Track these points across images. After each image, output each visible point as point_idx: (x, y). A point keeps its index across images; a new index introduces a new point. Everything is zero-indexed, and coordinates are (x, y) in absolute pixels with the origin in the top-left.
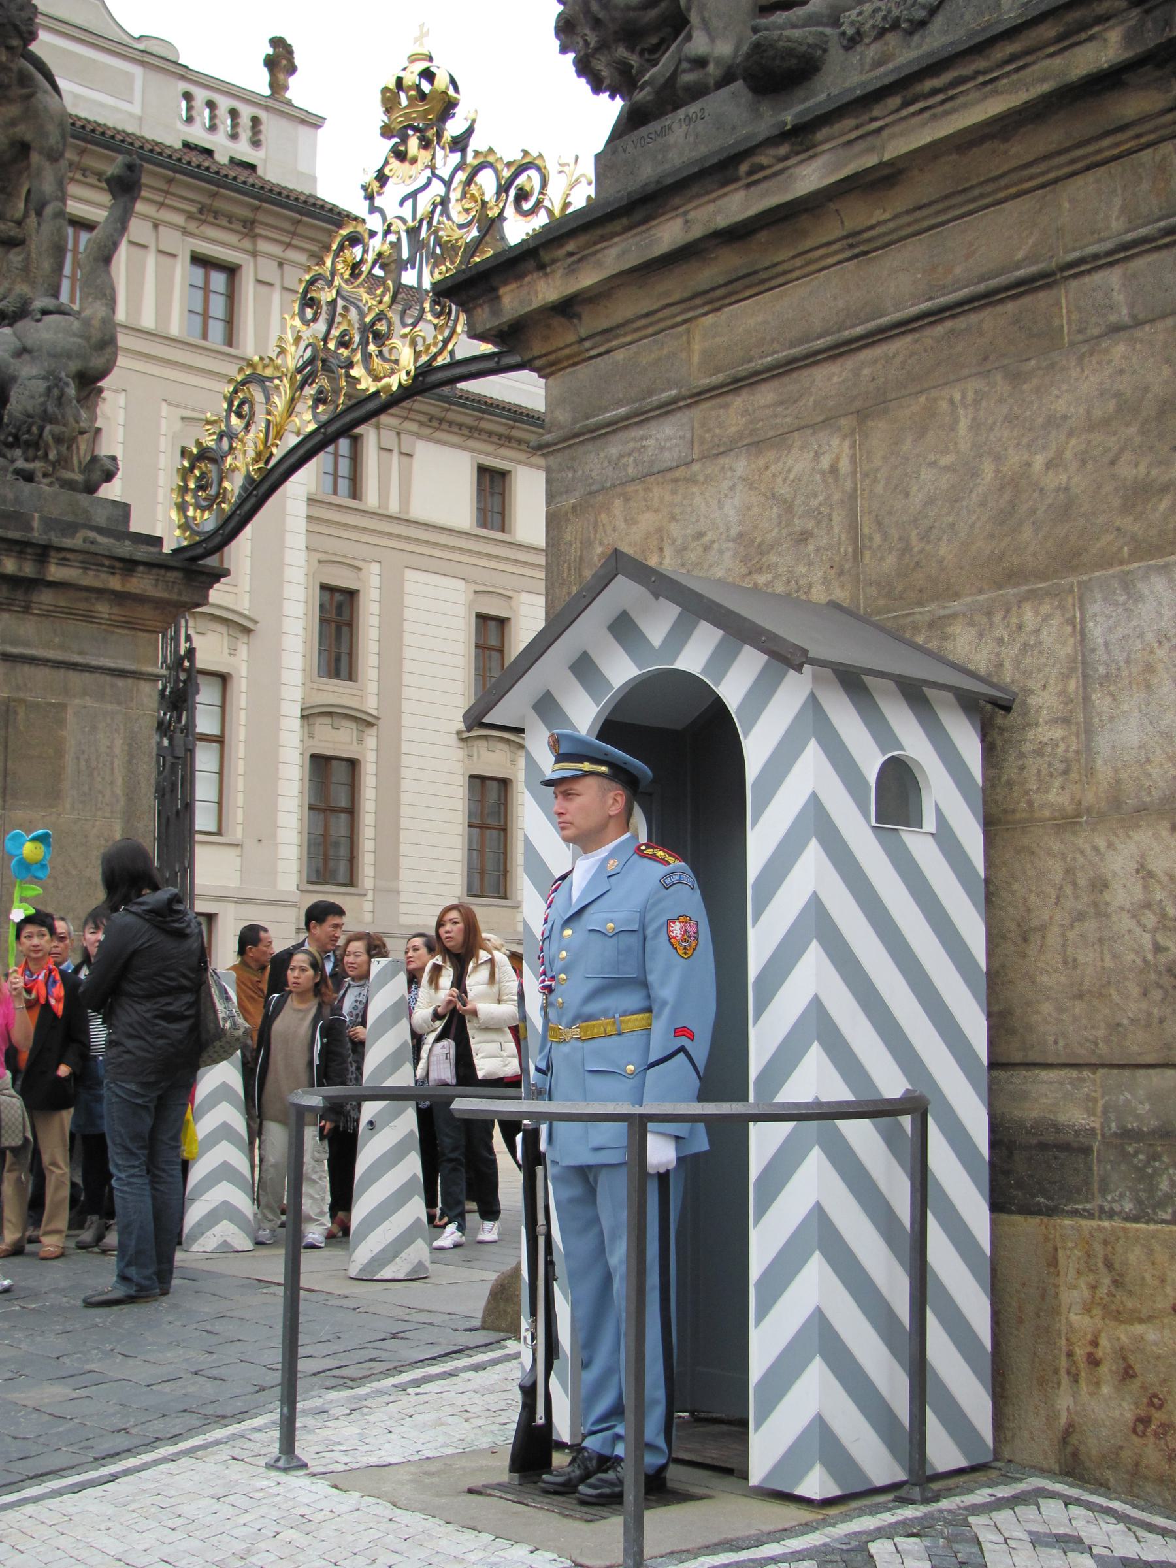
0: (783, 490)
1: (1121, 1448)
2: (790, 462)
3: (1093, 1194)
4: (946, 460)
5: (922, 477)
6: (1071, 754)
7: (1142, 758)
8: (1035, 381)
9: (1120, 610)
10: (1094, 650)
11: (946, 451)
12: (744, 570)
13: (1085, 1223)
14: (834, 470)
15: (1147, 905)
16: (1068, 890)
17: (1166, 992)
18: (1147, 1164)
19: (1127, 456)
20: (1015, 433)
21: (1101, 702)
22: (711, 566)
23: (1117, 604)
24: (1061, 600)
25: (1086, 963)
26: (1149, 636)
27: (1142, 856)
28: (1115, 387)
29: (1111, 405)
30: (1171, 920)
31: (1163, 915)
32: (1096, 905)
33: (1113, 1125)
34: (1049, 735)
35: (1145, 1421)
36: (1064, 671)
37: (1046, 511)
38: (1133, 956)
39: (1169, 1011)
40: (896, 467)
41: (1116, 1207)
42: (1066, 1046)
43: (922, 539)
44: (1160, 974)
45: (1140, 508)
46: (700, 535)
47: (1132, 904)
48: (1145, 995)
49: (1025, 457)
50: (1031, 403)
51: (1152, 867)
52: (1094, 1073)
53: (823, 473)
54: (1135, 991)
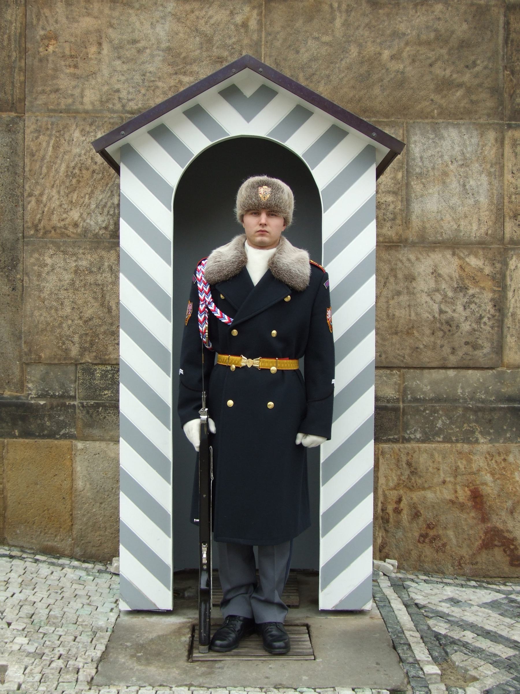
0: (207, 29)
1: (412, 550)
2: (210, 13)
3: (399, 431)
4: (326, 39)
5: (309, 44)
6: (397, 210)
7: (439, 218)
8: (386, 10)
9: (431, 141)
10: (414, 159)
11: (326, 33)
12: (170, 70)
13: (396, 446)
14: (245, 25)
15: (437, 290)
16: (392, 280)
17: (445, 333)
18: (431, 415)
19: (439, 63)
20: (372, 35)
21: (416, 186)
22: (143, 63)
23: (429, 138)
24: (395, 130)
25: (401, 317)
26: (446, 158)
27: (436, 266)
28: (435, 26)
29: (432, 35)
30: (450, 298)
31: (446, 296)
32: (408, 288)
33: (409, 396)
34: (384, 199)
35: (424, 536)
36: (395, 167)
37: (389, 81)
38: (427, 315)
39: (446, 342)
40: (291, 34)
41: (412, 436)
42: (387, 358)
43: (307, 79)
44: (442, 324)
45: (445, 92)
46: (134, 42)
47: (428, 289)
48: (433, 334)
49: (378, 49)
50: (384, 21)
51: (441, 272)
52: (399, 371)
53: (236, 25)
54: (428, 332)
